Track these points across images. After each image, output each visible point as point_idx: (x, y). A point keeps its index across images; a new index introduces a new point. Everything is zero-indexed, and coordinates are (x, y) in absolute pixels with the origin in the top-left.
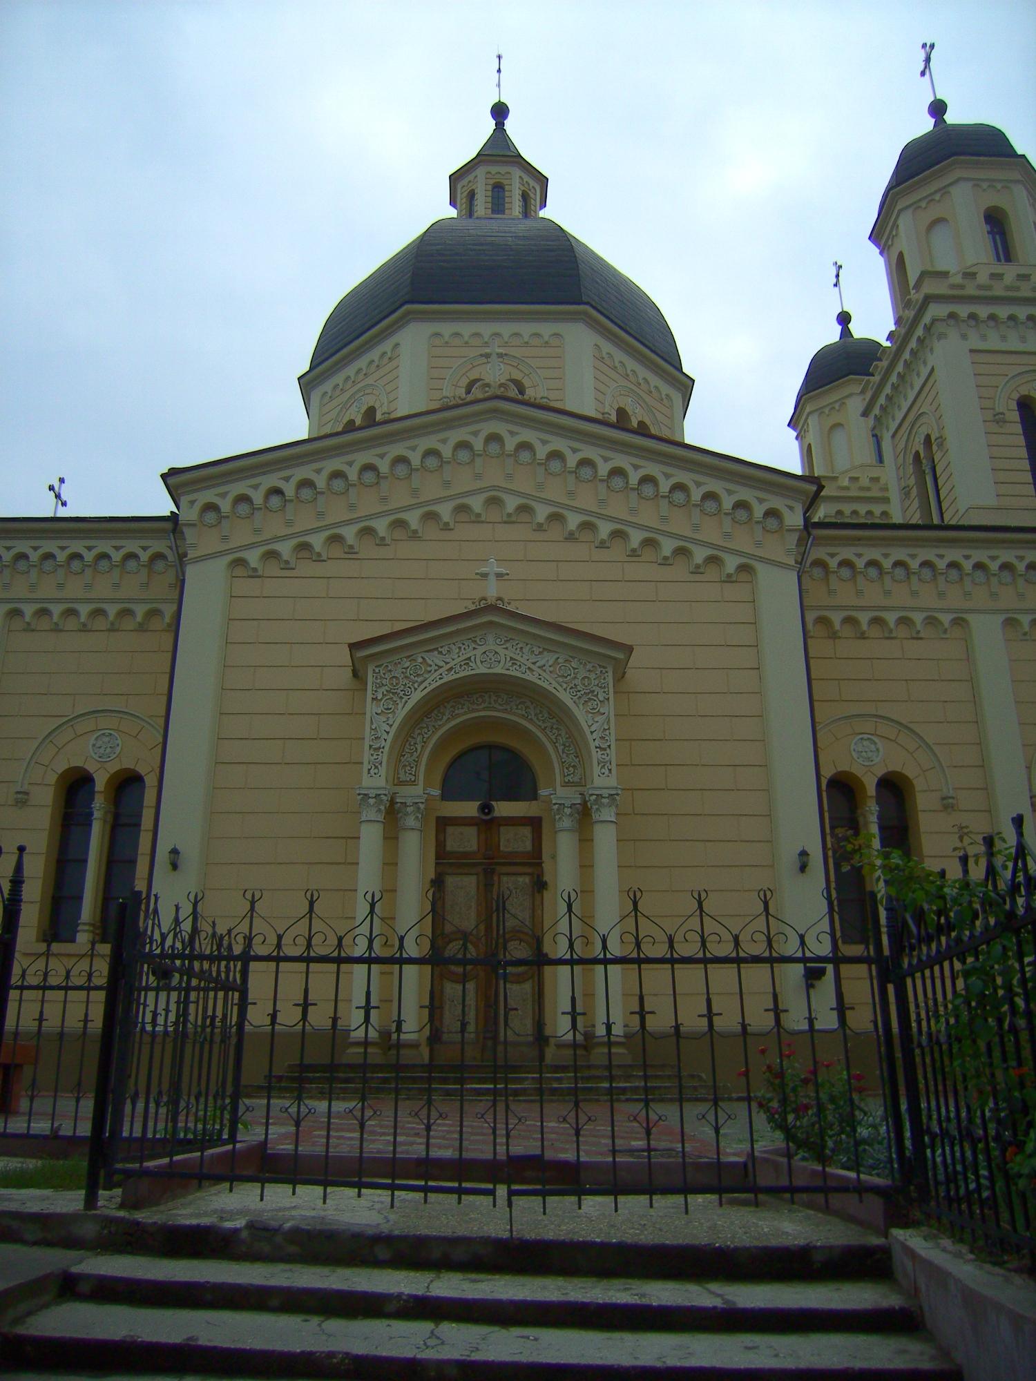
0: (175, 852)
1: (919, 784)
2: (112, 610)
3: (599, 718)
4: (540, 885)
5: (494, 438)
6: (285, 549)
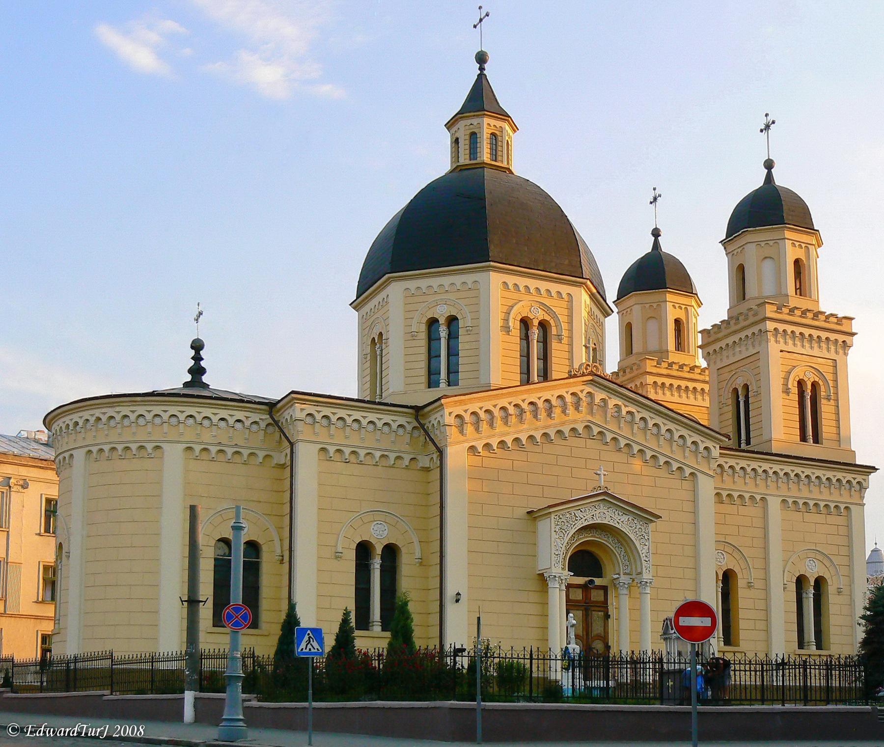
3: (646, 547)
4: (607, 616)
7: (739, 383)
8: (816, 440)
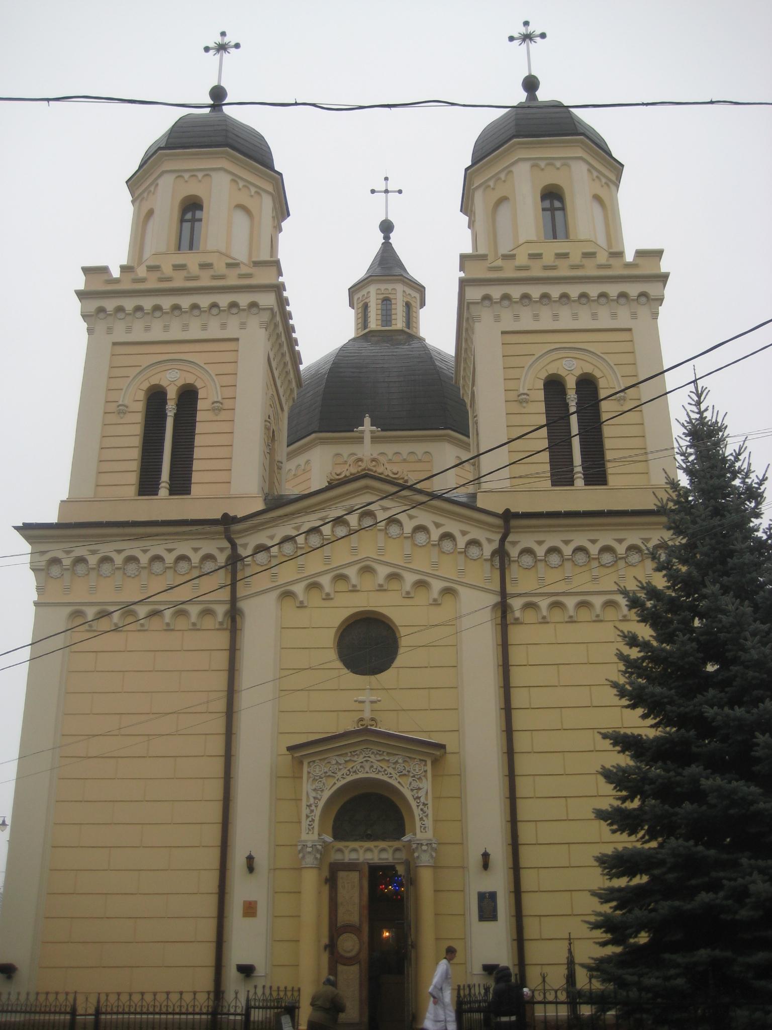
8: (596, 474)
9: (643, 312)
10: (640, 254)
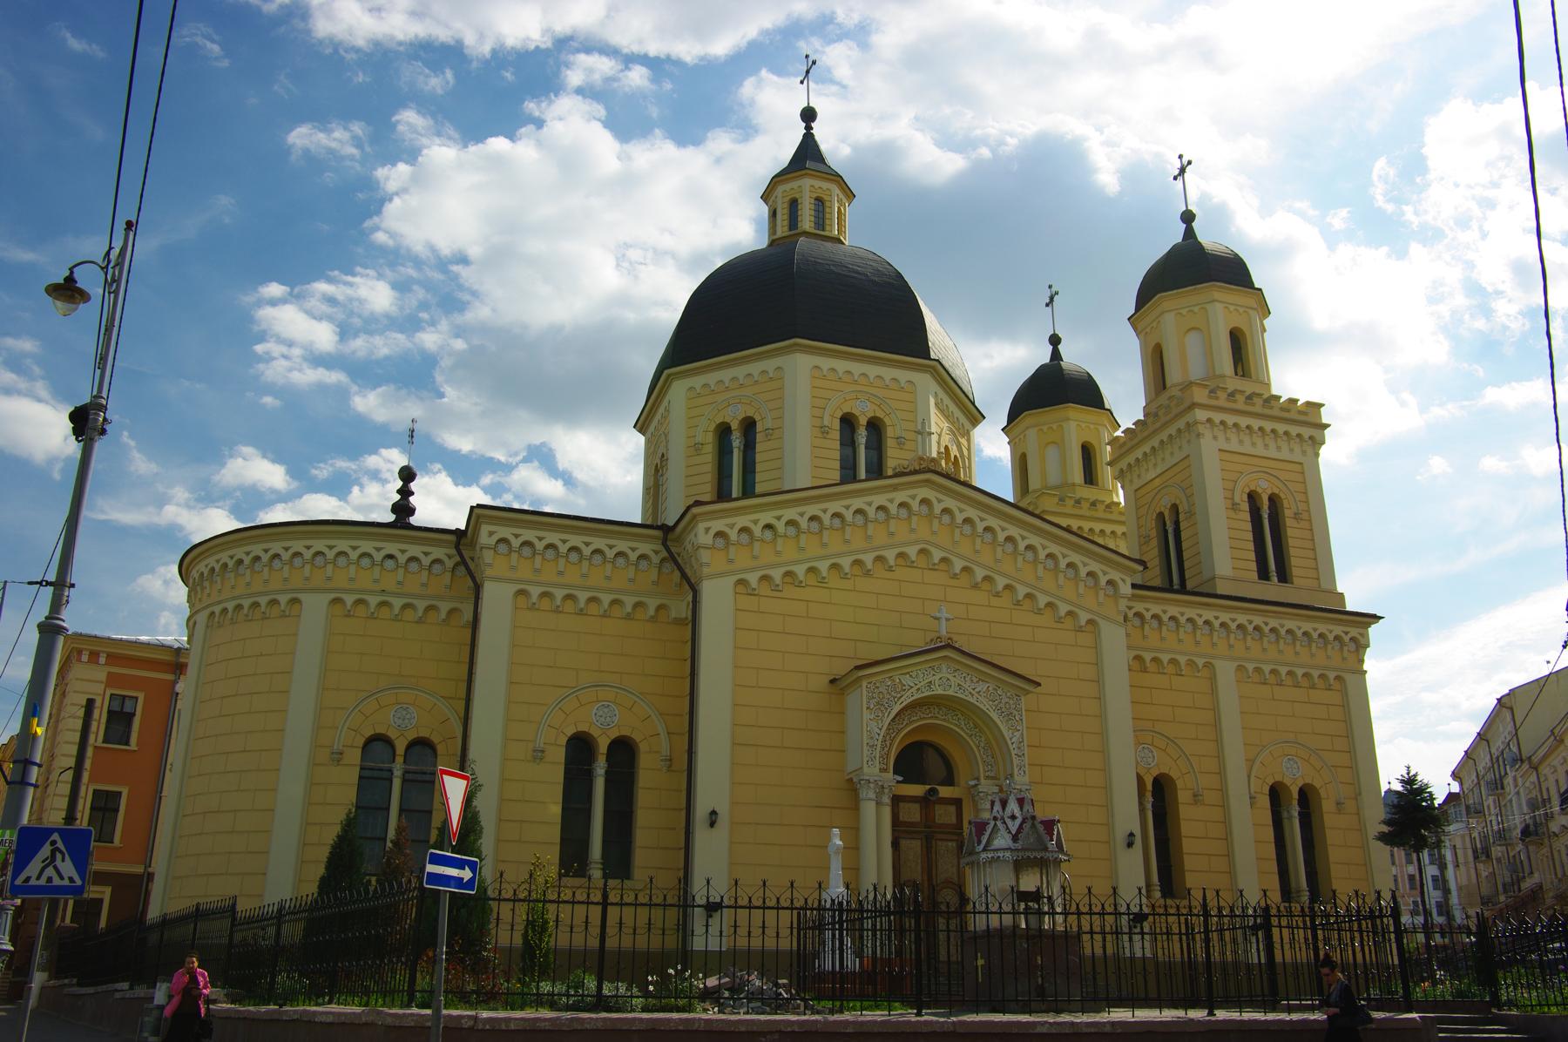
0: (714, 813)
1: (1179, 784)
2: (606, 599)
5: (924, 501)
6: (777, 574)
7: (1164, 505)
8: (1284, 577)
9: (1309, 451)
10: (1308, 404)
